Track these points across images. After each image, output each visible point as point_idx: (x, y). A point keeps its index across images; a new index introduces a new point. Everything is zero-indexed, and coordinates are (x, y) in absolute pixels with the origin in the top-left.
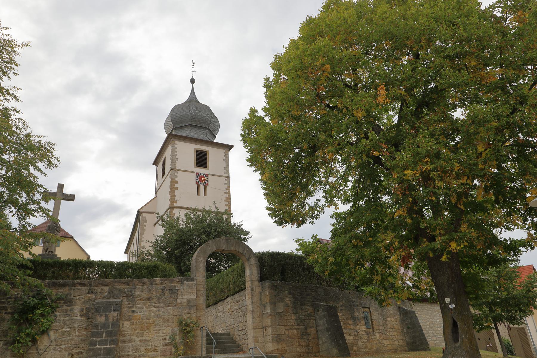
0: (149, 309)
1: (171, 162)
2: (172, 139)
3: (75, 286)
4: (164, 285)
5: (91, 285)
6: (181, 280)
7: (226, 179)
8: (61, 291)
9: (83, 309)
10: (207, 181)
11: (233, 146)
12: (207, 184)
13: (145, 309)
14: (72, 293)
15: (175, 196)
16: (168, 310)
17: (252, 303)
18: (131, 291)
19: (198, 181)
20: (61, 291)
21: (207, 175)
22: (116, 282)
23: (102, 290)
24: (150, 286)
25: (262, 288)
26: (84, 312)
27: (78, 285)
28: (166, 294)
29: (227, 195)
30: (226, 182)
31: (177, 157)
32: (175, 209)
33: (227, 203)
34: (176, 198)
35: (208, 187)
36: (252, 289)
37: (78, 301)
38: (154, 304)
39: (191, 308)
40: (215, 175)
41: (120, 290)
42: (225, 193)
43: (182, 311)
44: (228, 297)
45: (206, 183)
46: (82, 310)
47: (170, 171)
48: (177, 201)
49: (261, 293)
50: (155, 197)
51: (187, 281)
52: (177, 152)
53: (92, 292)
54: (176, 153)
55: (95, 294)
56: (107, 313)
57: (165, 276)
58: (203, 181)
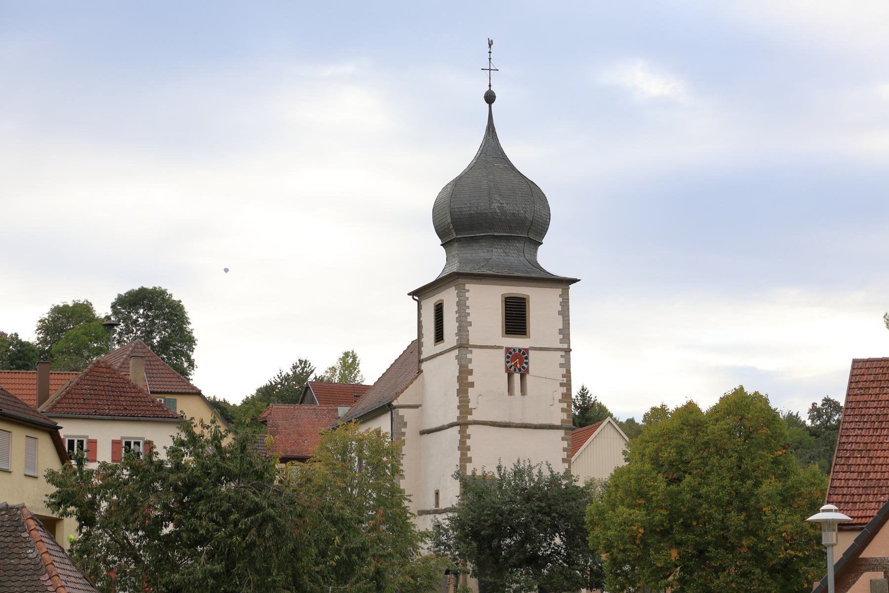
7: (563, 353)
12: (527, 371)
15: (468, 401)
19: (509, 364)
21: (526, 351)
29: (564, 390)
30: (563, 361)
31: (469, 319)
32: (469, 426)
34: (471, 406)
42: (562, 385)
45: (524, 368)
48: (473, 410)
54: (467, 311)
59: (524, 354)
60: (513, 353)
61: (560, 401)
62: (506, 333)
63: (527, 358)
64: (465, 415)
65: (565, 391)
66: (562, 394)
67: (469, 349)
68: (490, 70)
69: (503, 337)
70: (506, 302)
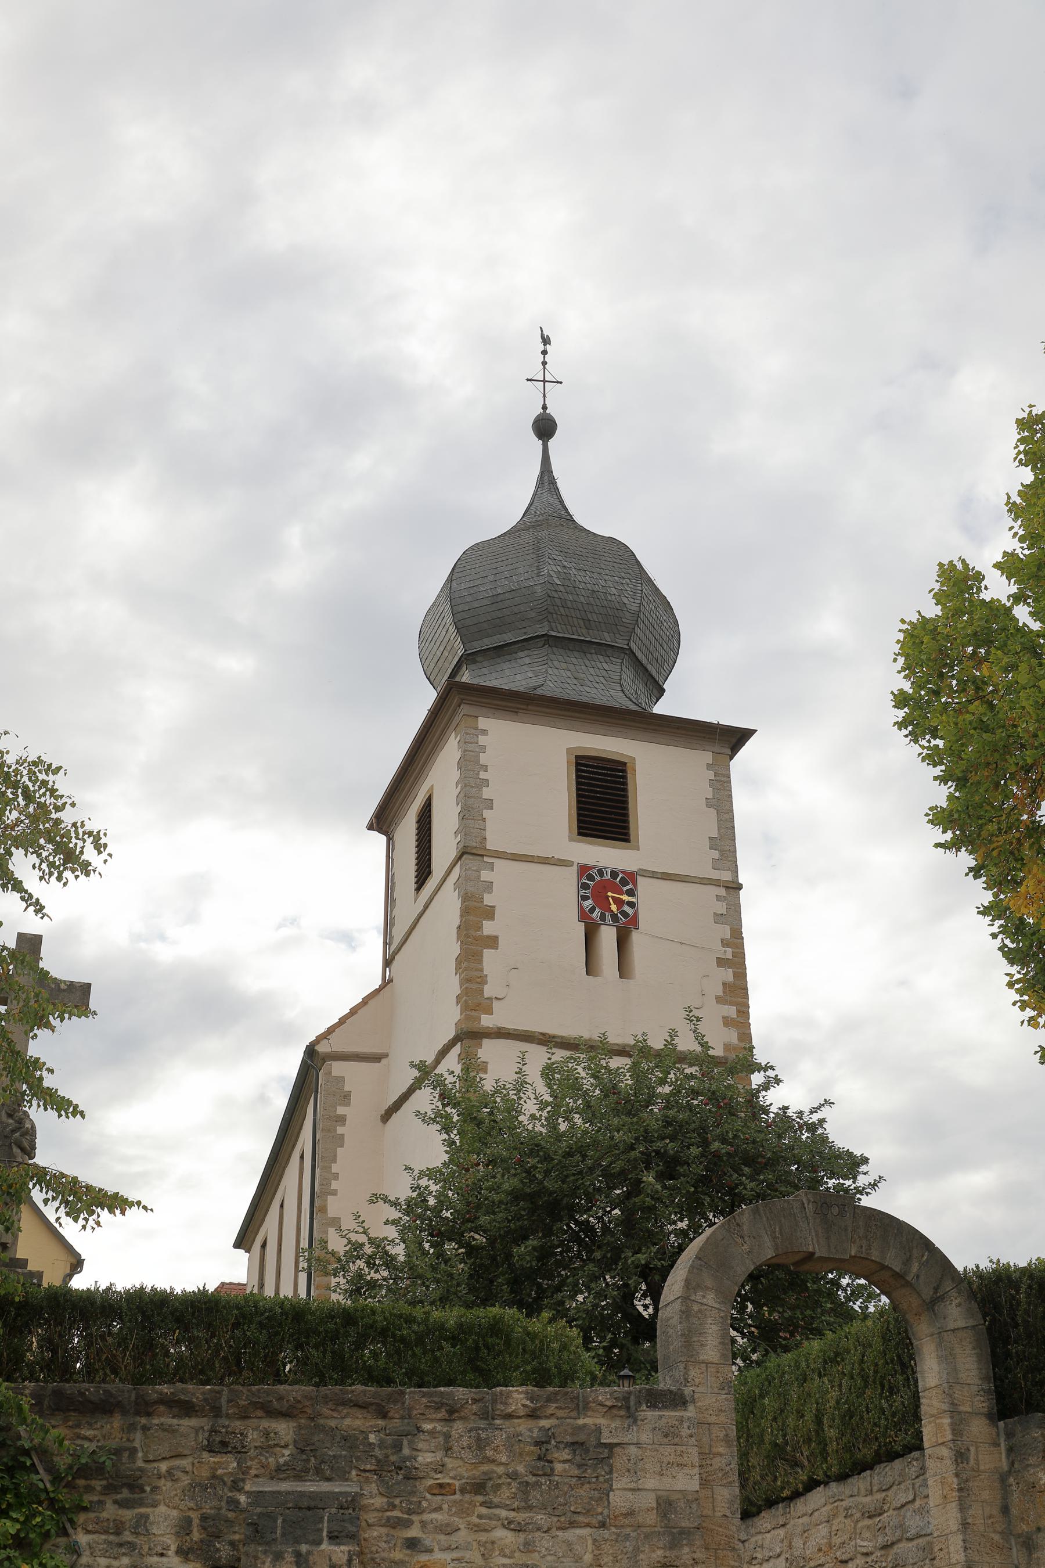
0: (483, 1537)
1: (463, 817)
2: (465, 709)
3: (149, 1414)
4: (545, 1423)
5: (216, 1412)
6: (626, 1399)
7: (722, 892)
8: (89, 1433)
9: (189, 1521)
10: (631, 905)
11: (751, 732)
12: (634, 922)
13: (463, 1535)
14: (137, 1444)
15: (483, 980)
16: (569, 1544)
17: (965, 1525)
18: (398, 1447)
19: (588, 904)
20: (89, 1433)
22: (326, 1399)
23: (267, 1434)
24: (482, 1424)
25: (1010, 1450)
26: (196, 1535)
27: (162, 1408)
28: (559, 1467)
29: (728, 975)
30: (721, 908)
31: (486, 793)
32: (486, 1042)
33: (732, 1011)
34: (488, 991)
35: (636, 937)
36: (960, 1456)
37: (165, 1485)
38: (504, 1513)
39: (677, 1537)
40: (666, 877)
41: (349, 1441)
42: (721, 962)
43: (637, 1550)
44: (812, 1485)
45: (625, 914)
46: (184, 1527)
47: (459, 858)
48: (495, 1004)
49: (1003, 1479)
50: (386, 983)
51: (653, 1406)
52: (485, 768)
53: (224, 1444)
54: (483, 775)
55: (240, 1452)
56: (304, 1548)
57: (540, 1378)
58: (614, 907)
59: (624, 882)
60: (598, 878)
61: (719, 1000)
62: (580, 834)
63: (631, 893)
64: (473, 1013)
65: (730, 978)
66: (724, 984)
67: (486, 859)
68: (544, 381)
69: (571, 840)
70: (577, 764)
